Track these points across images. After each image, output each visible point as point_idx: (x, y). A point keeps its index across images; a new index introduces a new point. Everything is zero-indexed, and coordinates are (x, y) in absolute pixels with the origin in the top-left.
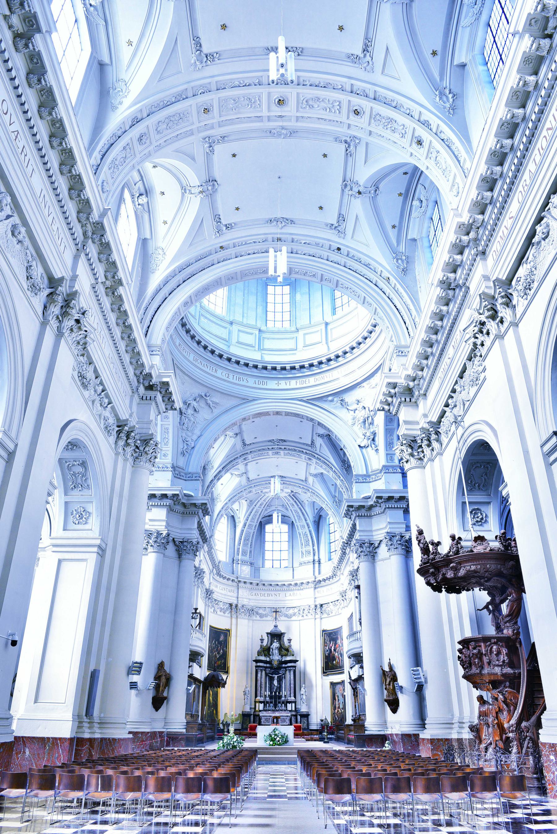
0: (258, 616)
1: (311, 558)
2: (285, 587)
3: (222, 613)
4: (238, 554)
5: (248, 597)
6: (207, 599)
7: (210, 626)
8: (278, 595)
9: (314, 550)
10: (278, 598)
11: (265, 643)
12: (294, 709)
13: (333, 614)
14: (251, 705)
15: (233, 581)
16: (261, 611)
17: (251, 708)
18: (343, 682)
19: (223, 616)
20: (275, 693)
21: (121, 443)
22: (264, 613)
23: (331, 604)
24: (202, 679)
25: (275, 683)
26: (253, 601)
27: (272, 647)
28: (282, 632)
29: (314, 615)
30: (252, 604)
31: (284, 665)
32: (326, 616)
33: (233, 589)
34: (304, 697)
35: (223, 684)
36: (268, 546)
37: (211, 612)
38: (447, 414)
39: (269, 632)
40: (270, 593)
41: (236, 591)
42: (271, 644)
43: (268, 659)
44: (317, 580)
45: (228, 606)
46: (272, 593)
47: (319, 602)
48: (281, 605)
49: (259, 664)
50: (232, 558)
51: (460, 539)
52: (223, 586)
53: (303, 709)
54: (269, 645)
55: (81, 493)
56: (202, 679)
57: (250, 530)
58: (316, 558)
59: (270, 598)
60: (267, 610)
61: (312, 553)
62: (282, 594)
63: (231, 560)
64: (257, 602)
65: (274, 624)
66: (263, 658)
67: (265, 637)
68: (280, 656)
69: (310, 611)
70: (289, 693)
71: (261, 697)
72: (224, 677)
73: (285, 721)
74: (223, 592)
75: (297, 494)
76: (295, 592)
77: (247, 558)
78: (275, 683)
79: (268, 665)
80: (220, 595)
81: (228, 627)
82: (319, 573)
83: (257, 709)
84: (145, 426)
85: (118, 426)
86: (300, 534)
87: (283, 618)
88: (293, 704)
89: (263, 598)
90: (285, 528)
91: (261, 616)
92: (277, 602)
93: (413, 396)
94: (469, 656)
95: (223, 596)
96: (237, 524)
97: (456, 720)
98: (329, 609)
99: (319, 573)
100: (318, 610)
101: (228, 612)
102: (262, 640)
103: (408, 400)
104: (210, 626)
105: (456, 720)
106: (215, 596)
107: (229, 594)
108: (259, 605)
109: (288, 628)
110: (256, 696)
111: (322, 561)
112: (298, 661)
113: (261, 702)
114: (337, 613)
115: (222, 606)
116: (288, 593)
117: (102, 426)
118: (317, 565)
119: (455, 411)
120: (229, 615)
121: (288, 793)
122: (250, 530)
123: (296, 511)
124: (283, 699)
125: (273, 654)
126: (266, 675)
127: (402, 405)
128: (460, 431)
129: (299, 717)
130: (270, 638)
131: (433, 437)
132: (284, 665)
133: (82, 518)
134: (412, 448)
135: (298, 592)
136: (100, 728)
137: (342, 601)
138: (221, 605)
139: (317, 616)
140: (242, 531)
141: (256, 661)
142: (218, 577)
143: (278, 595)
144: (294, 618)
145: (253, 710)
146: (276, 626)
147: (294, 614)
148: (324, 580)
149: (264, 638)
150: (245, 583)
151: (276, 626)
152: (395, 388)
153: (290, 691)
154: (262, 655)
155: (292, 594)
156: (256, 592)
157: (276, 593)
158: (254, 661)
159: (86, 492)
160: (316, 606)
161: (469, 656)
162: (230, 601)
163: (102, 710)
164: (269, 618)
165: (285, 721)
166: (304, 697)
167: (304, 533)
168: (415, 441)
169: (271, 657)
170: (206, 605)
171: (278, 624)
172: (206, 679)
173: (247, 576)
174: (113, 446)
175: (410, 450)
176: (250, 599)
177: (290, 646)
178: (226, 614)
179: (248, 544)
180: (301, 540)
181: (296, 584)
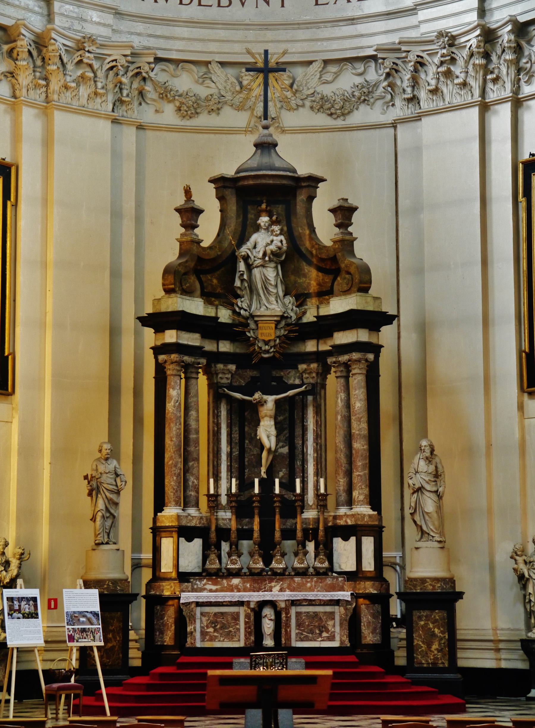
0: (169, 109)
12: (369, 565)
14: (137, 547)
17: (137, 565)
22: (203, 91)
26: (140, 27)
27: (244, 250)
28: (302, 171)
29: (475, 85)
30: (137, 42)
31: (310, 346)
39: (230, 171)
42: (242, 239)
54: (230, 238)
64: (160, 30)
68: (289, 300)
69: (457, 70)
70: (342, 481)
71: (186, 505)
73: (323, 628)
79: (225, 347)
88: (368, 543)
110: (159, 506)
124: (310, 514)
125: (252, 289)
126: (211, 385)
130: (232, 207)
132: (310, 346)
145: (147, 575)
149: (198, 202)
153: (349, 474)
154: (187, 292)
165: (323, 628)
169: (243, 303)
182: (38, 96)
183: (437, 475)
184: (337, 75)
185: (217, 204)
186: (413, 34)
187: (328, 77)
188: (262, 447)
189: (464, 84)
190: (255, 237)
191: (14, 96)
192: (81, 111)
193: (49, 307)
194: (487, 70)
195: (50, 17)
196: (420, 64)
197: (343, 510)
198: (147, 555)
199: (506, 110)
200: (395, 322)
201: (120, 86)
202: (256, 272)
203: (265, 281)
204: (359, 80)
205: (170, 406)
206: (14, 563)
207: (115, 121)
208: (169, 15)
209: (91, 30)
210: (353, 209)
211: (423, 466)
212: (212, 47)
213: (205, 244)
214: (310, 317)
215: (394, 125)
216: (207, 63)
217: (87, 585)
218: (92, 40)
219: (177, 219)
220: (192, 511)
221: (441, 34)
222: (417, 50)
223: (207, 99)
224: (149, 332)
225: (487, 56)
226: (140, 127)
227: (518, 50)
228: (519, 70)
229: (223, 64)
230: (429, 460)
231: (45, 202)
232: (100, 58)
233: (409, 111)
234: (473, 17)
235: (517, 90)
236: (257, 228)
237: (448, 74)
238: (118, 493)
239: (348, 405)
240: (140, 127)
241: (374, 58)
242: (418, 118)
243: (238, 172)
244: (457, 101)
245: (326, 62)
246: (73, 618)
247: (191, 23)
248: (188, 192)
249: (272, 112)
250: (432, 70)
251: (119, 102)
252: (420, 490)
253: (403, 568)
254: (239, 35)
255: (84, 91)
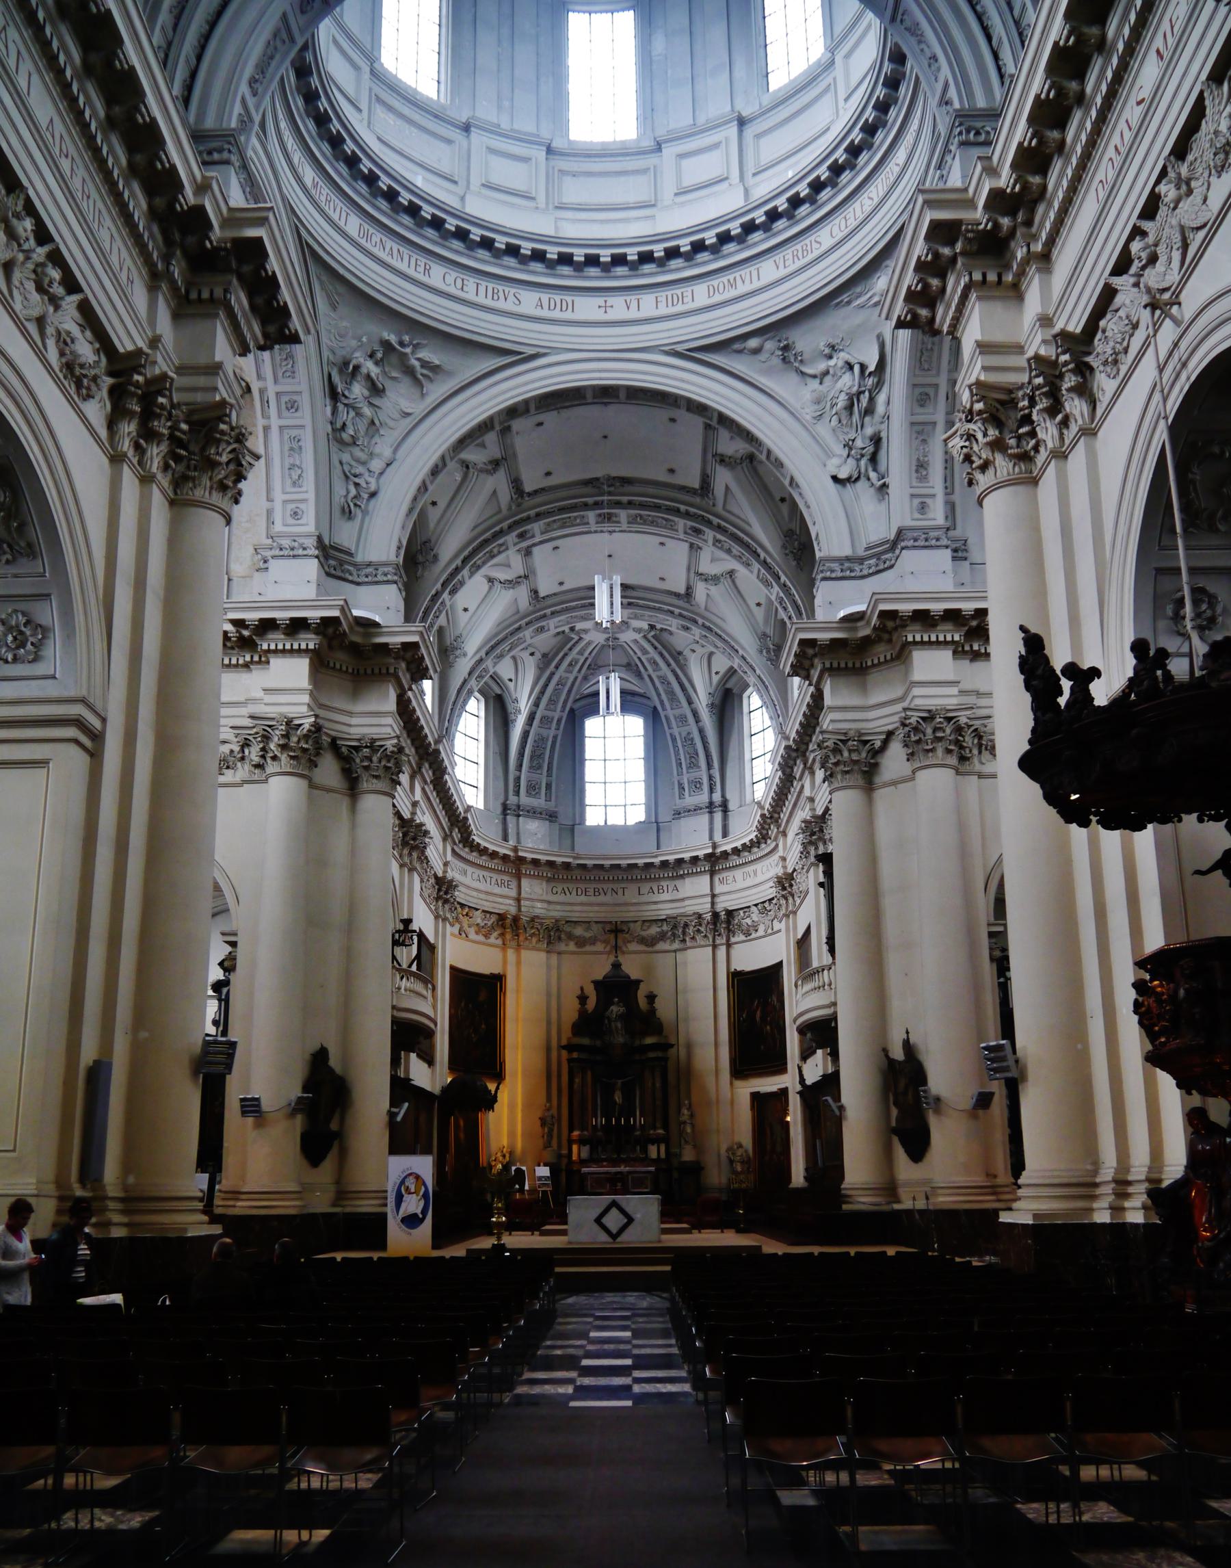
1: (703, 798)
2: (638, 874)
3: (481, 938)
4: (517, 793)
5: (544, 897)
6: (440, 903)
7: (452, 968)
8: (620, 892)
9: (711, 778)
10: (620, 898)
11: (591, 1004)
12: (663, 1155)
13: (761, 932)
14: (560, 1146)
15: (505, 858)
16: (579, 931)
17: (560, 1156)
18: (784, 1092)
19: (484, 944)
20: (618, 1121)
21: (129, 428)
22: (587, 935)
23: (754, 909)
24: (437, 1090)
25: (618, 1097)
26: (558, 907)
27: (607, 1013)
28: (634, 976)
32: (742, 937)
33: (506, 878)
34: (689, 1130)
35: (490, 1102)
36: (592, 771)
37: (452, 934)
38: (1118, 300)
39: (600, 977)
40: (600, 886)
41: (514, 884)
43: (598, 1043)
44: (719, 850)
45: (494, 918)
46: (605, 886)
47: (723, 904)
48: (630, 914)
49: (575, 1055)
50: (501, 799)
51: (1163, 654)
52: (482, 873)
53: (688, 1155)
55: (12, 570)
56: (437, 1090)
57: (544, 732)
58: (717, 797)
59: (601, 899)
60: (595, 927)
61: (706, 787)
62: (632, 889)
63: (499, 809)
65: (612, 959)
66: (586, 1041)
67: (591, 992)
69: (702, 929)
71: (582, 1130)
72: (492, 1087)
74: (481, 886)
75: (665, 635)
76: (664, 884)
77: (539, 802)
78: (618, 1097)
80: (475, 894)
81: (496, 972)
82: (725, 834)
83: (575, 1157)
84: (202, 381)
85: (111, 374)
86: (674, 739)
87: (633, 947)
88: (663, 1147)
89: (583, 898)
90: (636, 724)
91: (581, 942)
92: (617, 908)
93: (1008, 267)
94: (1174, 996)
95: (483, 896)
96: (512, 717)
97: (1108, 1172)
98: (748, 921)
99: (725, 834)
100: (722, 927)
101: (495, 934)
102: (583, 998)
103: (992, 277)
104: (452, 968)
105: (1108, 1172)
106: (460, 895)
107: (497, 890)
108: (575, 916)
109: (649, 969)
110: (571, 1130)
111: (731, 806)
112: (672, 1046)
113: (582, 1142)
114: (770, 931)
115: (479, 921)
116: (645, 888)
117: (53, 355)
118: (718, 816)
119: (1153, 278)
120: (499, 942)
121: (638, 1381)
122: (544, 732)
123: (664, 680)
124: (638, 1133)
127: (973, 296)
128: (1168, 332)
129: (676, 1175)
131: (1070, 381)
133: (23, 645)
134: (999, 424)
135: (671, 884)
136: (124, 1212)
137: (783, 902)
138: (478, 918)
139: (721, 940)
140: (525, 734)
141: (569, 1048)
142: (467, 850)
143: (620, 892)
144: (662, 946)
145: (565, 1161)
146: (616, 966)
147: (662, 937)
148: (736, 851)
150: (535, 862)
151: (616, 966)
152: (951, 243)
155: (656, 892)
156: (565, 886)
157: (615, 886)
158: (564, 1047)
159: (24, 566)
160: (715, 915)
161: (1174, 996)
162: (500, 909)
163: (128, 1165)
164: (599, 947)
166: (689, 1130)
167: (684, 734)
168: (1012, 403)
170: (437, 917)
171: (621, 959)
172: (446, 1090)
173: (541, 847)
174: (103, 433)
175: (993, 433)
176: (549, 902)
177: (653, 1011)
178: (492, 940)
179: (540, 767)
180: (677, 753)
181: (665, 864)
182: (514, 944)
183: (692, 1116)
184: (649, 927)
185: (595, 992)
186: (682, 911)
187: (645, 928)
188: (615, 1102)
189: (705, 936)
190: (612, 1007)
191: (504, 944)
192: (534, 949)
193: (520, 1039)
194: (715, 930)
195: (519, 907)
196: (686, 925)
197: (652, 1132)
198: (565, 1152)
199: (724, 948)
200: (676, 1047)
201: (550, 936)
202: (613, 1024)
203: (616, 1027)
204: (658, 930)
205: (576, 1086)
206: (507, 1156)
207: (548, 952)
208: (572, 901)
209: (538, 912)
210: (655, 996)
211: (686, 1112)
212: (591, 915)
213: (590, 1011)
214: (637, 1043)
215: (675, 951)
216: (589, 922)
217: (545, 1165)
218: (538, 917)
219: (577, 1001)
220: (586, 1133)
221: (694, 913)
222: (685, 919)
223: (590, 938)
224: (564, 1053)
225: (715, 924)
226: (559, 953)
227: (728, 922)
228: (729, 931)
229: (596, 922)
230: (688, 1109)
231: (518, 991)
232: (541, 924)
233: (682, 946)
234: (709, 906)
235: (728, 940)
236: (613, 1004)
237: (699, 931)
238: (553, 1125)
239: (654, 1084)
240: (559, 953)
241: (665, 920)
242: (685, 949)
243: (604, 977)
244: (702, 943)
245: (644, 921)
246: (540, 1178)
247: (582, 904)
248: (582, 989)
249: (620, 943)
250: (691, 928)
251: (549, 943)
252: (685, 1123)
253: (680, 1155)
254: (603, 909)
255: (534, 940)
